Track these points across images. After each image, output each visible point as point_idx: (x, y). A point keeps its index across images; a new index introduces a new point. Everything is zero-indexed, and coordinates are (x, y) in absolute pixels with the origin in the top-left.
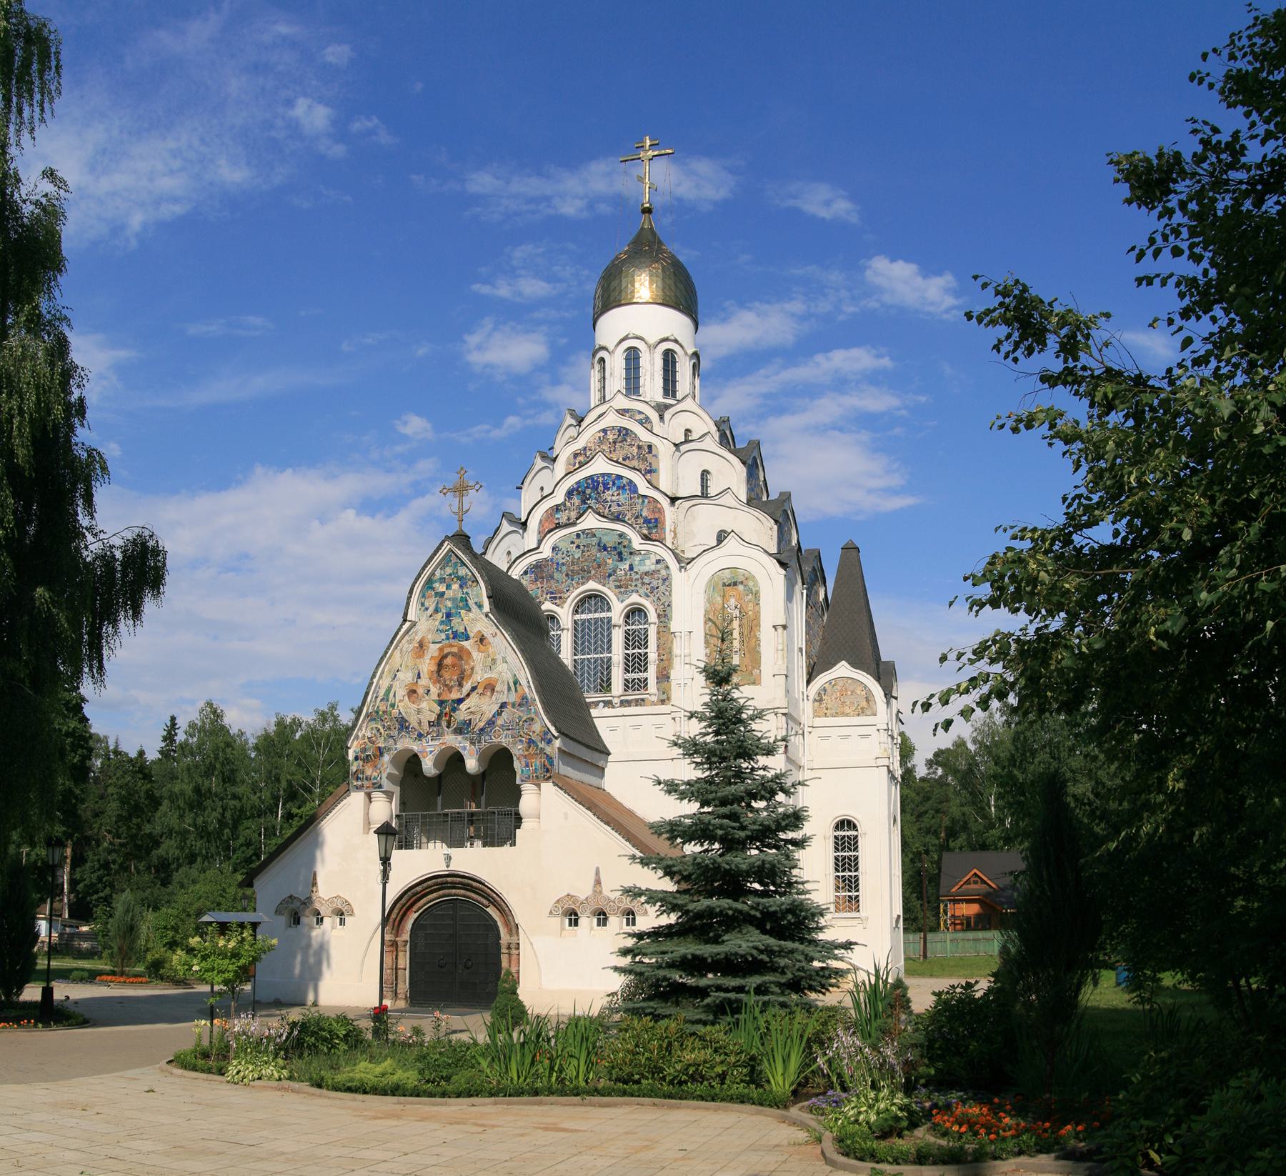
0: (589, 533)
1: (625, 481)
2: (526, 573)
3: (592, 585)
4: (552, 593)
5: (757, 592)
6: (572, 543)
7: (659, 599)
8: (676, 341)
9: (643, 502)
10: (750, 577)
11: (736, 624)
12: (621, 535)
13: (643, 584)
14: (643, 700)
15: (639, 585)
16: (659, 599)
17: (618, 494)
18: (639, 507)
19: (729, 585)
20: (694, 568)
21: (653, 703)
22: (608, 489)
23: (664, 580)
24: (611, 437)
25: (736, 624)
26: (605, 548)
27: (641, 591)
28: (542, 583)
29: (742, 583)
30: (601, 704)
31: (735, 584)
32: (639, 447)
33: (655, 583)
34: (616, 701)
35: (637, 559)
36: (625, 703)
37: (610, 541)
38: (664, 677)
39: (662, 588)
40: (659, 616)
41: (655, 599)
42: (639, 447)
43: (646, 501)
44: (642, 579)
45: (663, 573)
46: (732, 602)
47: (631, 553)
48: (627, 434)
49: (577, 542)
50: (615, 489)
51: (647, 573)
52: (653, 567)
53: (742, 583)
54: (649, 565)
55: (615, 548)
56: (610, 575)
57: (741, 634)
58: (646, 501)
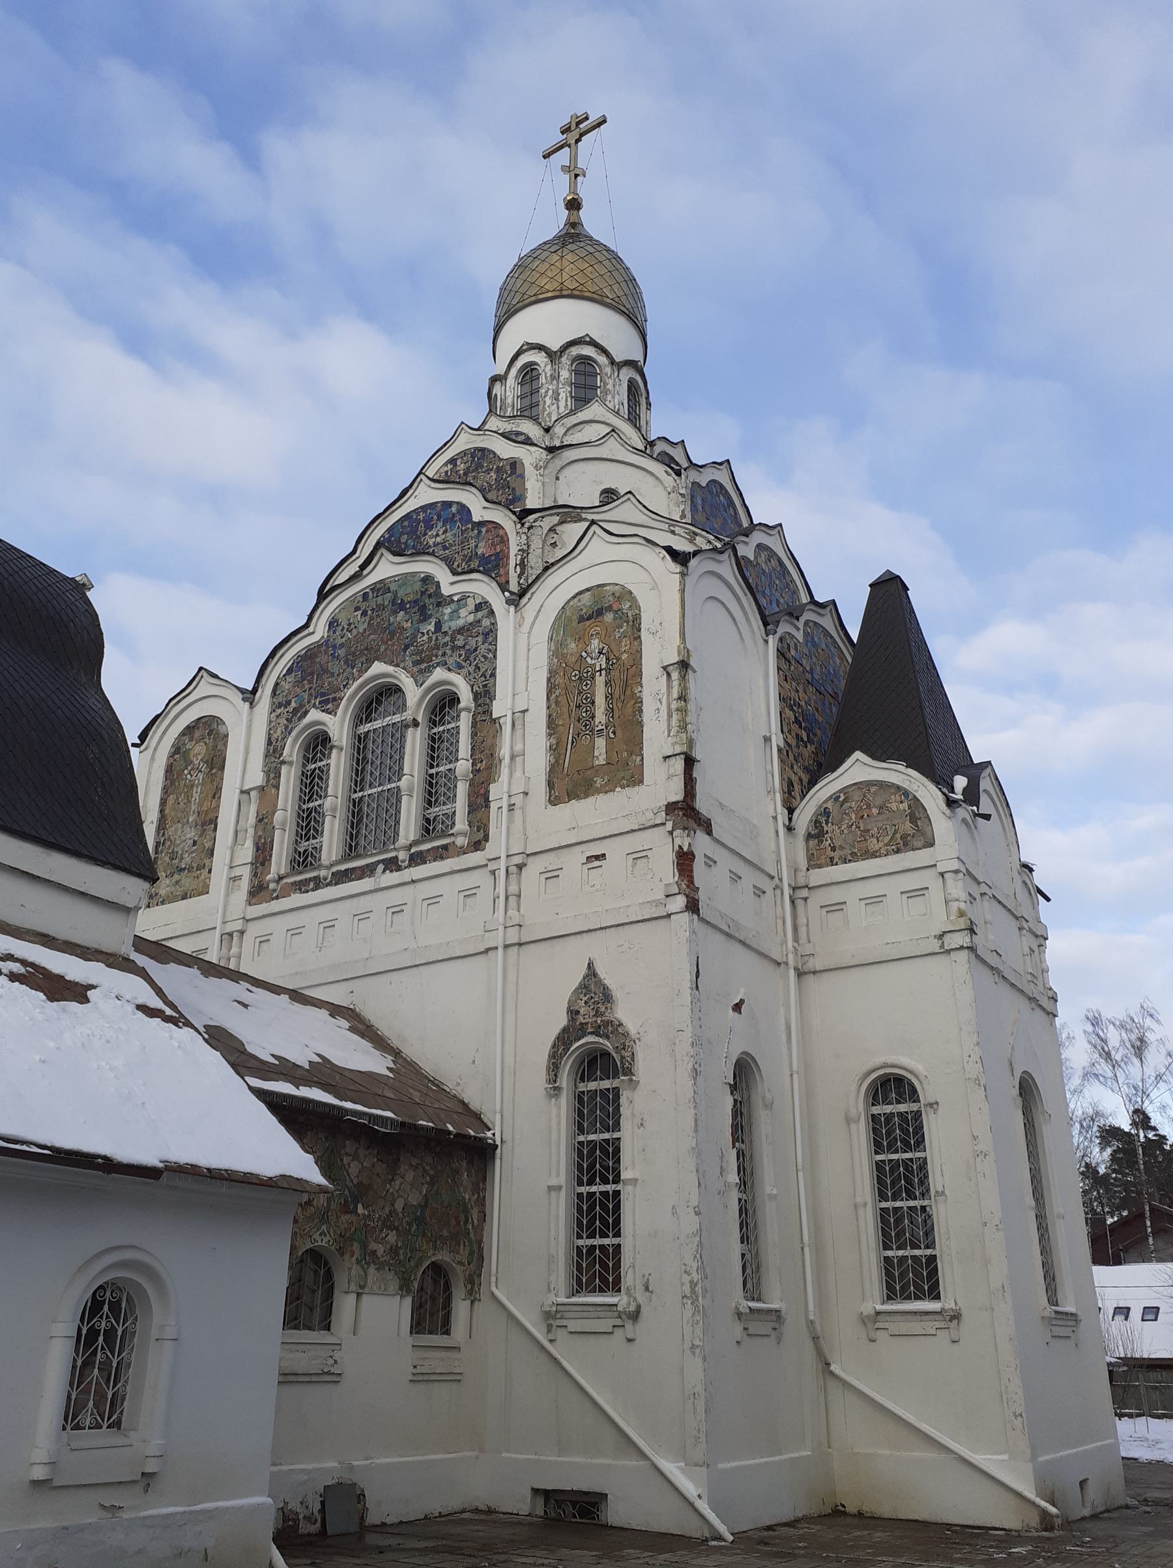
0: (381, 588)
1: (454, 509)
2: (290, 671)
3: (378, 668)
4: (323, 695)
5: (637, 618)
6: (357, 609)
7: (477, 668)
8: (593, 343)
9: (480, 532)
10: (625, 594)
11: (600, 680)
12: (428, 579)
13: (454, 648)
14: (445, 847)
15: (449, 652)
16: (477, 668)
17: (445, 532)
18: (472, 543)
19: (589, 619)
20: (531, 605)
21: (463, 851)
22: (431, 528)
23: (486, 635)
24: (461, 467)
25: (600, 680)
26: (402, 607)
27: (451, 661)
28: (310, 682)
29: (610, 608)
30: (381, 867)
31: (600, 612)
32: (499, 470)
33: (472, 643)
34: (402, 855)
35: (448, 610)
36: (417, 859)
37: (407, 593)
38: (479, 802)
39: (483, 649)
40: (476, 698)
41: (471, 669)
42: (499, 470)
43: (484, 530)
44: (453, 639)
45: (486, 622)
46: (595, 644)
47: (439, 604)
48: (483, 457)
49: (363, 606)
50: (440, 524)
51: (460, 631)
52: (471, 618)
53: (610, 608)
54: (466, 616)
55: (416, 602)
56: (407, 647)
57: (609, 697)
58: (484, 530)
